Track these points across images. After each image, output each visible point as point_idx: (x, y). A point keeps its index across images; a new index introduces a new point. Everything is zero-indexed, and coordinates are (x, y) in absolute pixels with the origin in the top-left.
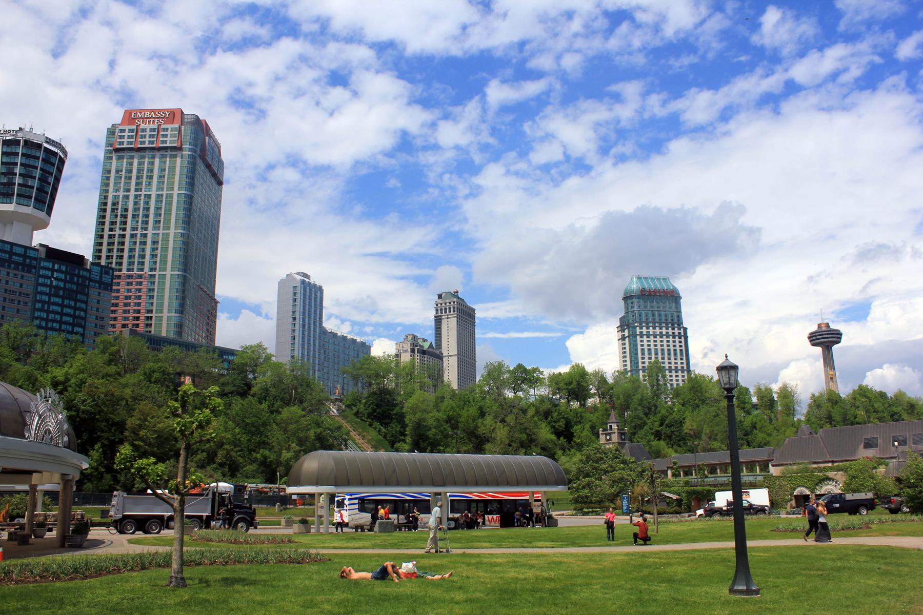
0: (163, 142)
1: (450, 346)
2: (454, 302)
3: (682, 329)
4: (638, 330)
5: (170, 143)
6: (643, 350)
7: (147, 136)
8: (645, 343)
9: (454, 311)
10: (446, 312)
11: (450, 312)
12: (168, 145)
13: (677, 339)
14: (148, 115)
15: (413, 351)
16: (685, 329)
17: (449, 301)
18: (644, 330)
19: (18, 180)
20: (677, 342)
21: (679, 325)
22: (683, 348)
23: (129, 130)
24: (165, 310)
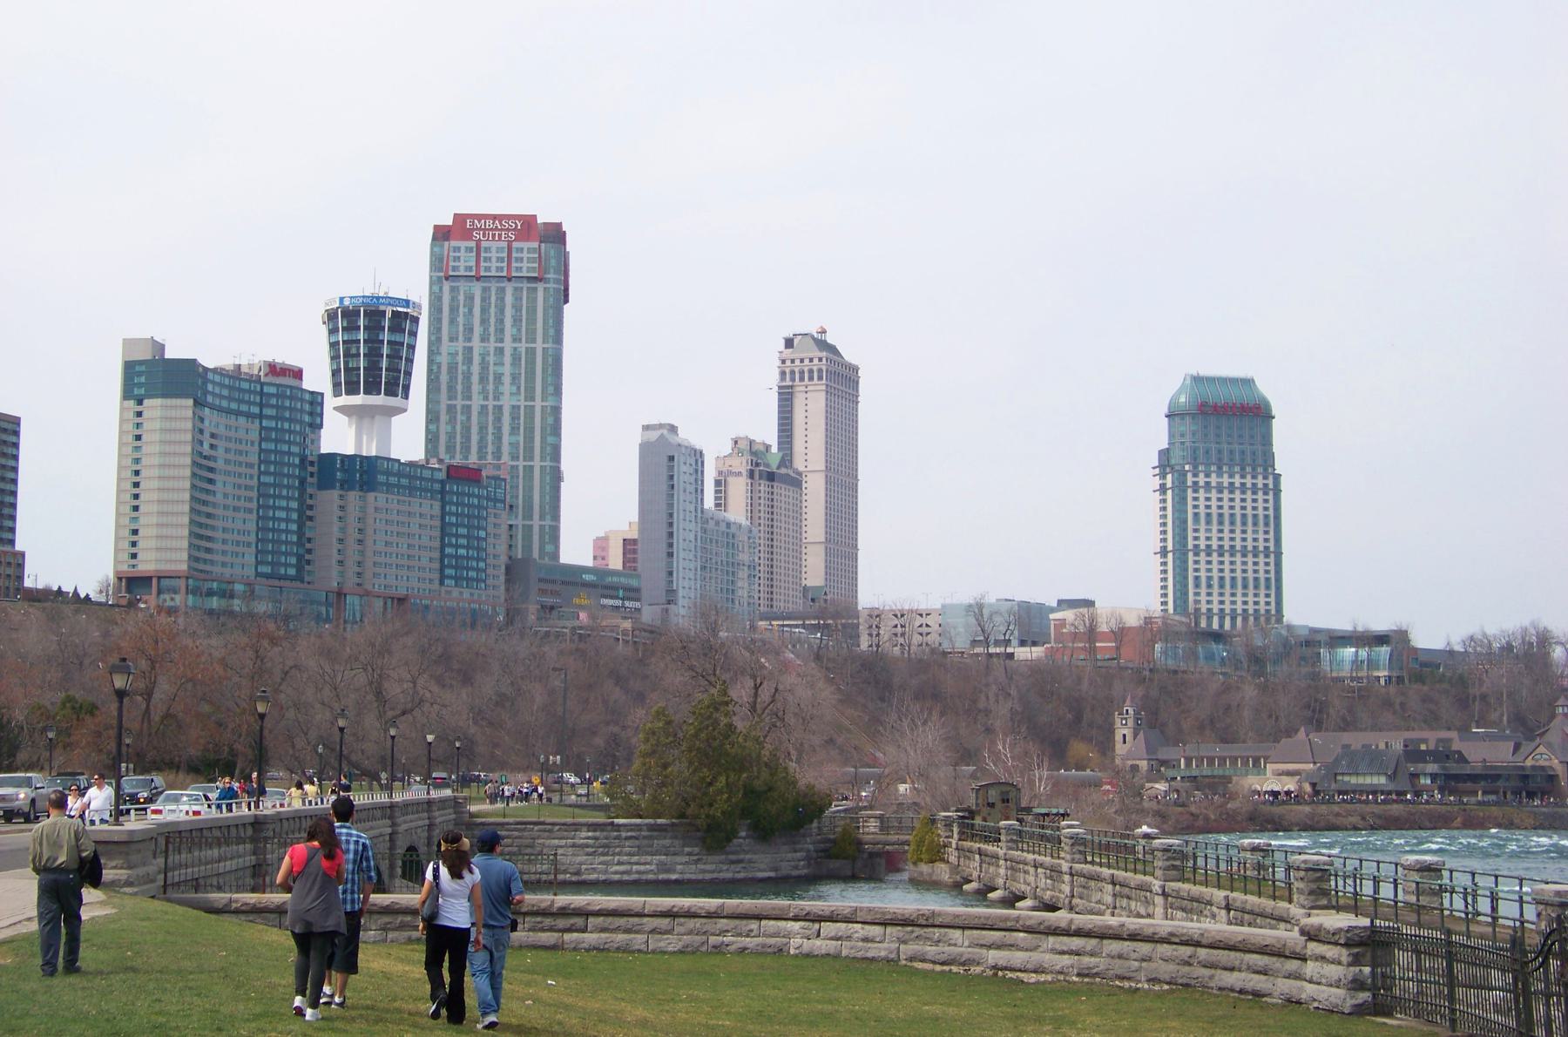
1: (811, 454)
2: (820, 360)
3: (1271, 477)
4: (1190, 479)
5: (528, 272)
6: (1196, 515)
7: (494, 260)
8: (1202, 503)
9: (820, 378)
10: (802, 379)
11: (811, 378)
12: (525, 274)
14: (490, 223)
15: (751, 474)
16: (1277, 477)
17: (811, 355)
18: (1202, 479)
20: (1260, 501)
21: (1266, 470)
23: (467, 248)
24: (536, 516)
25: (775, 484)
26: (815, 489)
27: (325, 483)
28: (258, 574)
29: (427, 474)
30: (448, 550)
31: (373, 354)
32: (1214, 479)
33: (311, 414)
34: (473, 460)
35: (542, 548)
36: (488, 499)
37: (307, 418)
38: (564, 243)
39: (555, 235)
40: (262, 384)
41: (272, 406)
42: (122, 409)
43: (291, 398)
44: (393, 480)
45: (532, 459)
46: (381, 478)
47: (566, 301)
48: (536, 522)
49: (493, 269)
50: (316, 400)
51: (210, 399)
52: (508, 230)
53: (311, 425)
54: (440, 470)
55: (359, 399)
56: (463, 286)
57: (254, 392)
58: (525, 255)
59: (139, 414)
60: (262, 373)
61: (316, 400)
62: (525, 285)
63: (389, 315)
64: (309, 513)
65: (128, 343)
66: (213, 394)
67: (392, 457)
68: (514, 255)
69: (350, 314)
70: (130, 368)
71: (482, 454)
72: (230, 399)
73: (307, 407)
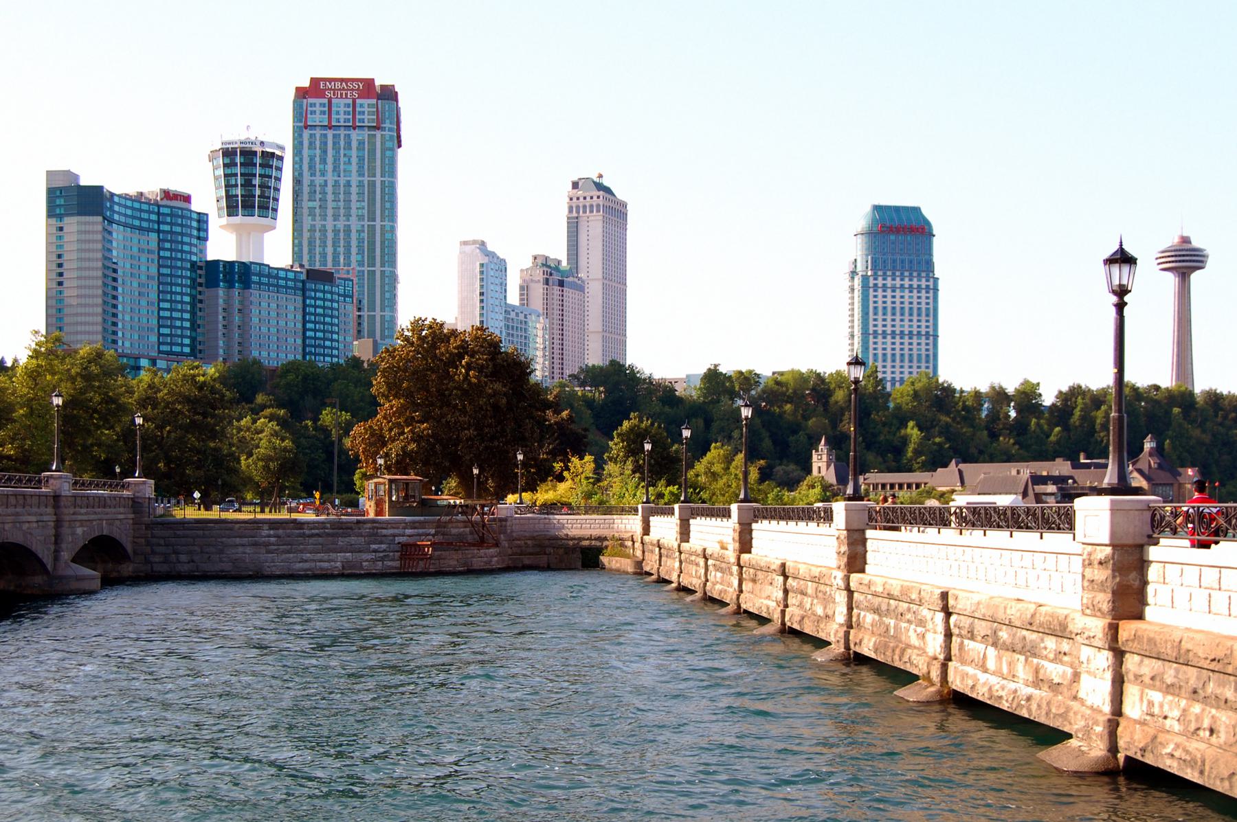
0: (360, 121)
2: (598, 197)
3: (932, 280)
6: (875, 308)
8: (880, 299)
9: (598, 211)
10: (585, 212)
11: (591, 211)
12: (366, 124)
13: (923, 294)
14: (338, 84)
15: (547, 282)
18: (880, 282)
19: (258, 192)
20: (924, 298)
22: (931, 306)
24: (378, 308)
25: (565, 289)
26: (595, 290)
27: (212, 283)
28: (160, 352)
29: (291, 275)
30: (309, 334)
31: (248, 184)
32: (889, 282)
33: (199, 230)
34: (329, 266)
35: (382, 331)
36: (339, 295)
37: (195, 233)
38: (397, 101)
39: (389, 94)
40: (159, 206)
41: (167, 223)
42: (48, 225)
43: (182, 217)
44: (265, 280)
45: (374, 265)
46: (255, 278)
47: (400, 146)
48: (378, 313)
49: (342, 120)
50: (202, 219)
51: (116, 217)
52: (352, 90)
53: (199, 238)
54: (302, 273)
55: (238, 219)
56: (318, 132)
57: (153, 212)
58: (366, 109)
59: (61, 229)
60: (159, 198)
61: (202, 219)
62: (366, 132)
63: (259, 154)
64: (199, 305)
65: (50, 174)
66: (119, 213)
67: (266, 263)
68: (358, 109)
69: (228, 153)
70: (53, 194)
71: (336, 261)
72: (133, 217)
73: (195, 224)
